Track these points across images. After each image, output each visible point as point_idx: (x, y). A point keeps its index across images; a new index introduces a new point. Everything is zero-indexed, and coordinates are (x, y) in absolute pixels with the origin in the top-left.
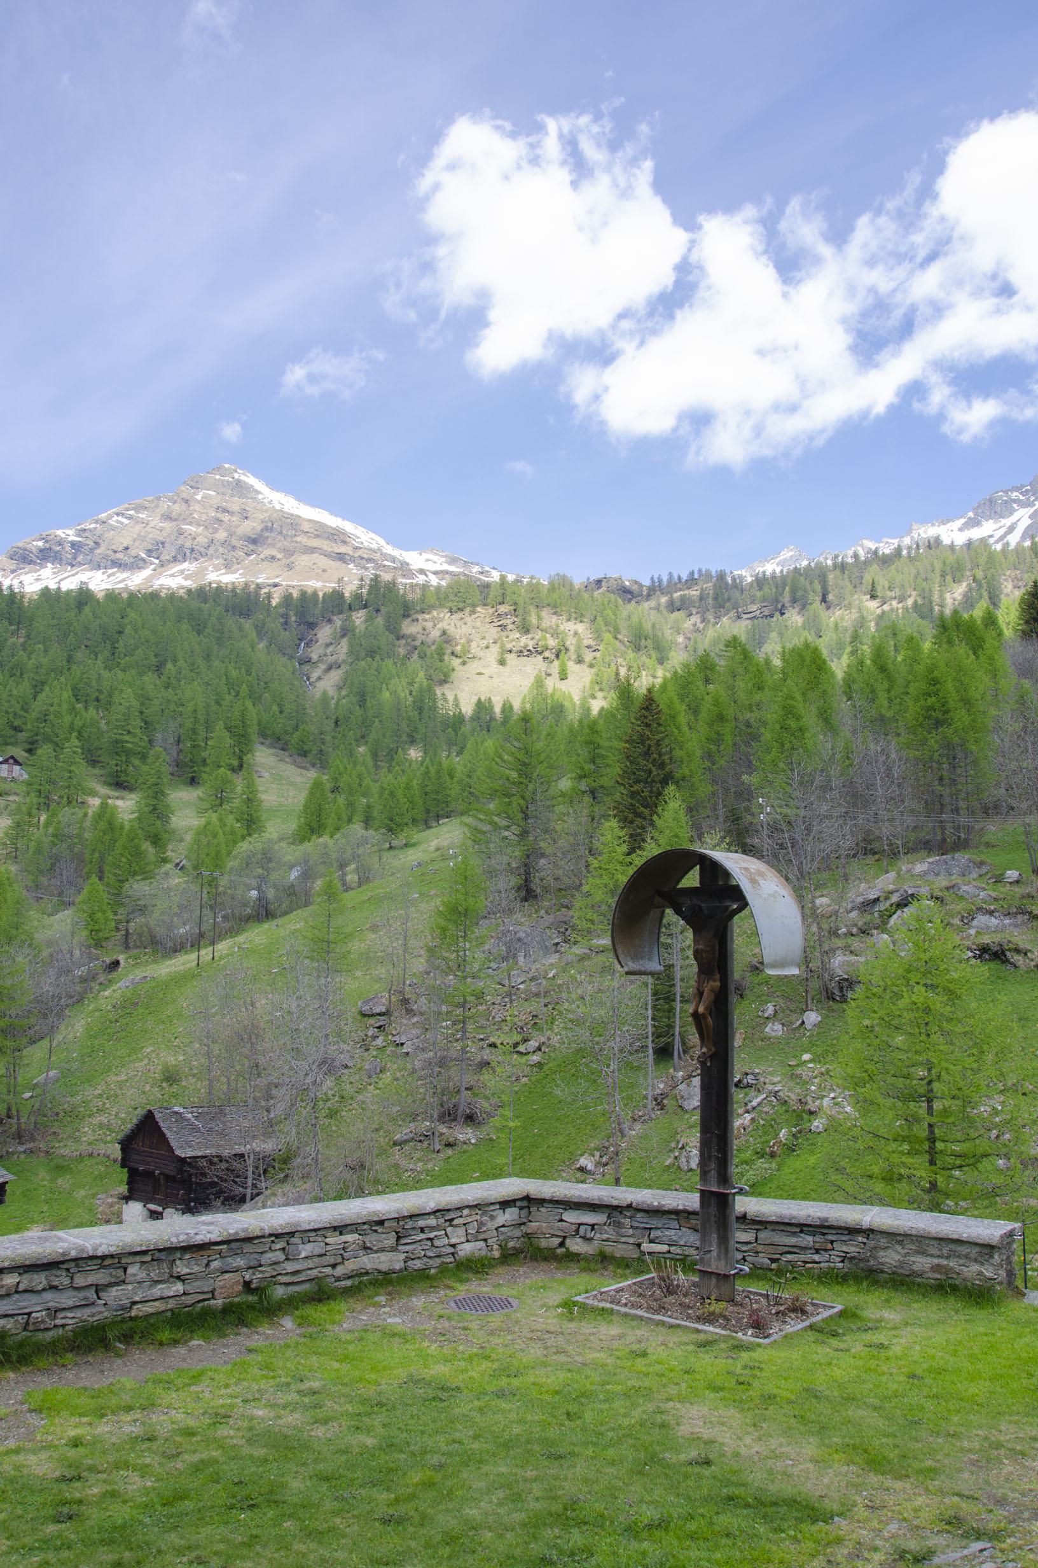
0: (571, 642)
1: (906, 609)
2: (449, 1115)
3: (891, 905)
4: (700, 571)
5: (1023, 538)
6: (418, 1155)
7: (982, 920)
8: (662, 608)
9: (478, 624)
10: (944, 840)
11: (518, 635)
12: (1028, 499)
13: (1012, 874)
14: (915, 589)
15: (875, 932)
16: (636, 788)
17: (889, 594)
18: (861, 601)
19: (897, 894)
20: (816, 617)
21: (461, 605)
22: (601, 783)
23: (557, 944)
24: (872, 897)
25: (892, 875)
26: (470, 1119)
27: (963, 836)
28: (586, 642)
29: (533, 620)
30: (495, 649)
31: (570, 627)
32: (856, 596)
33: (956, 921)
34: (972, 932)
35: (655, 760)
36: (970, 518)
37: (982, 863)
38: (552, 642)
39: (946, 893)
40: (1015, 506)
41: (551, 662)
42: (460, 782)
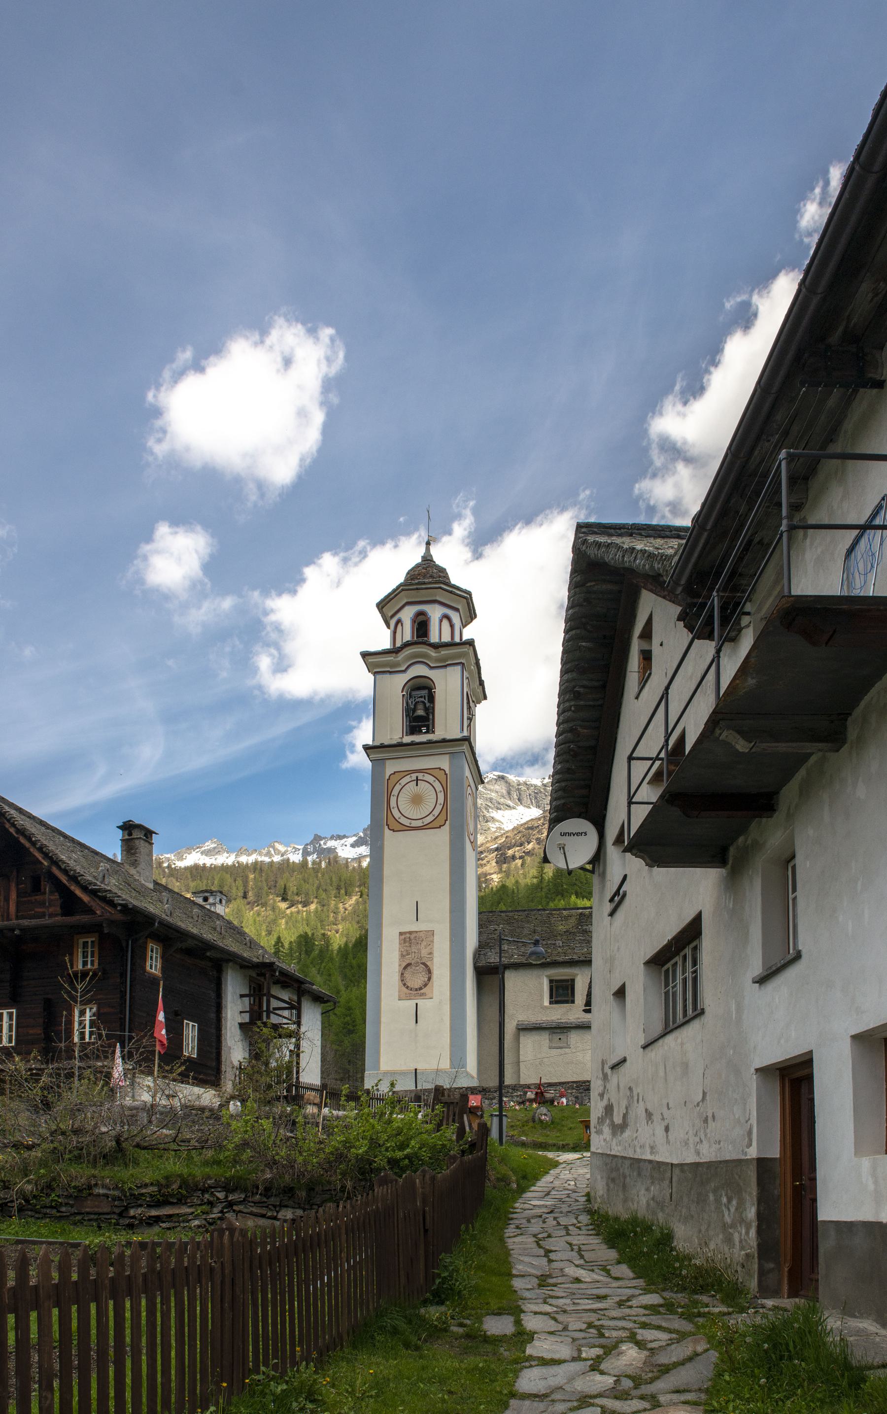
1: (308, 912)
14: (316, 897)
17: (296, 898)
18: (275, 901)
20: (239, 910)
32: (271, 897)
36: (360, 837)
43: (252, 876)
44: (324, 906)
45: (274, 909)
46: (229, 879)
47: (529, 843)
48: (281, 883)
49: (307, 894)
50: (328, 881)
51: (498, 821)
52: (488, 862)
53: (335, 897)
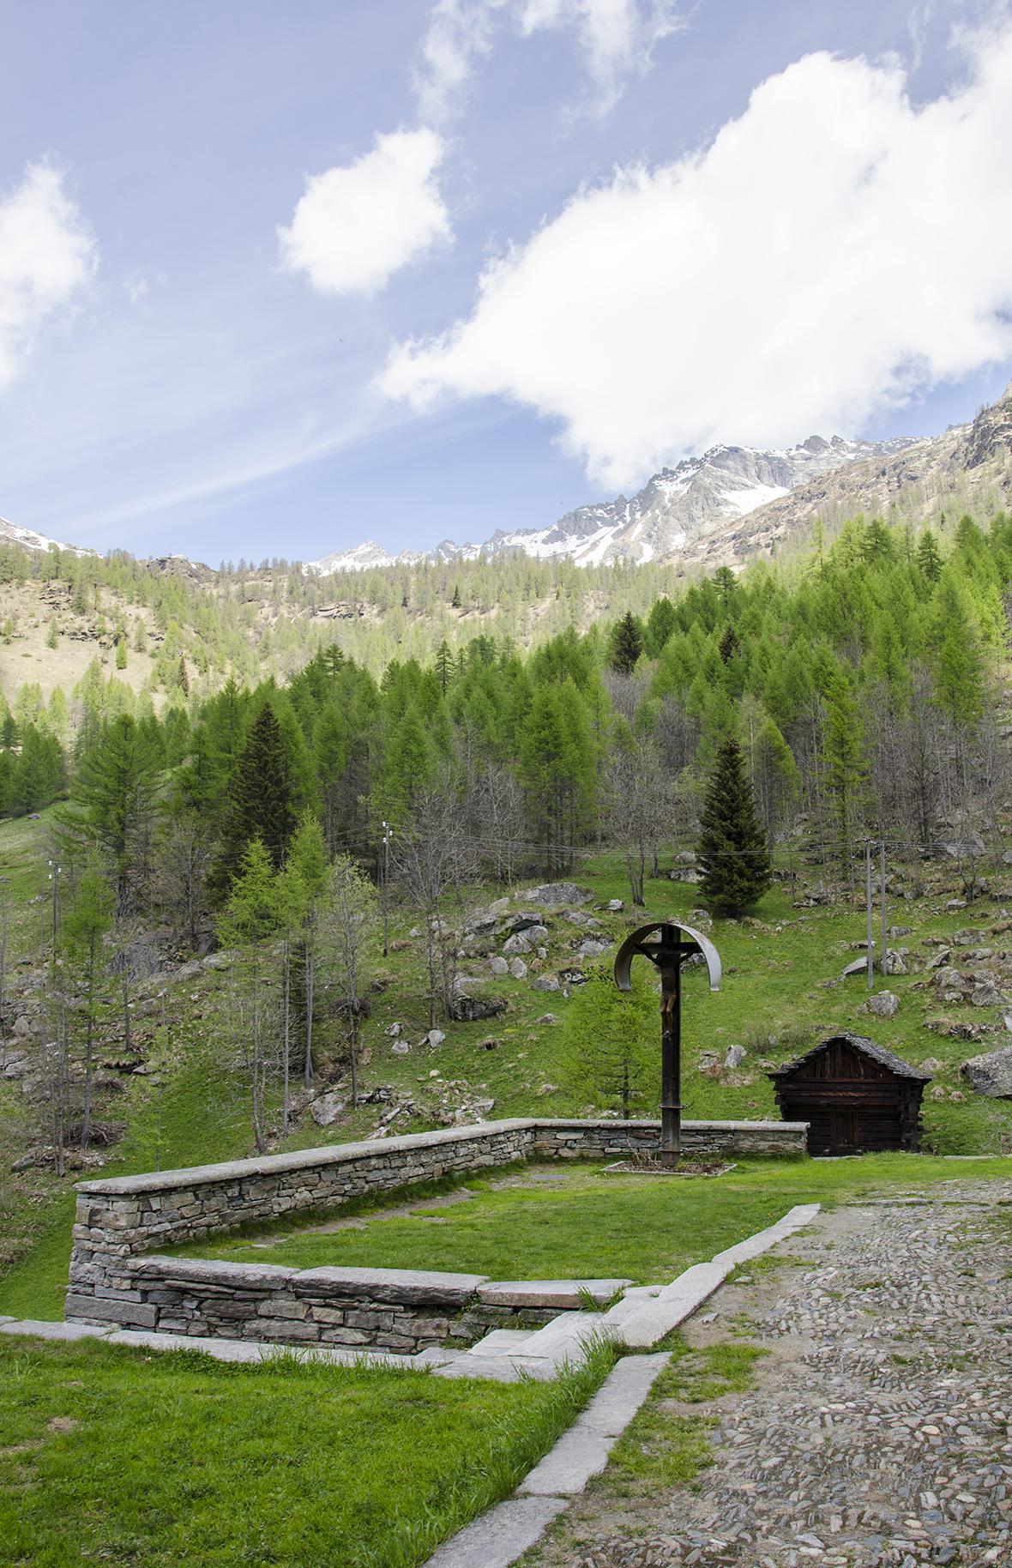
0: (132, 628)
1: (488, 621)
2: (73, 1139)
3: (507, 929)
4: (275, 560)
5: (605, 557)
6: (41, 1180)
7: (589, 945)
8: (231, 597)
9: (27, 599)
10: (550, 868)
11: (72, 616)
12: (612, 518)
13: (616, 903)
15: (491, 955)
16: (250, 804)
17: (472, 603)
18: (443, 608)
19: (513, 919)
20: (396, 621)
21: (8, 576)
22: (207, 796)
23: (162, 962)
24: (488, 921)
25: (505, 901)
26: (97, 1141)
27: (566, 863)
28: (149, 630)
29: (90, 599)
30: (46, 629)
31: (131, 610)
32: (438, 603)
33: (566, 946)
34: (581, 956)
35: (272, 776)
36: (554, 531)
37: (588, 891)
38: (110, 627)
39: (556, 919)
40: (599, 523)
41: (108, 649)
42: (17, 780)
43: (413, 579)
44: (508, 611)
45: (442, 618)
46: (383, 580)
47: (777, 527)
48: (451, 585)
49: (486, 597)
50: (514, 579)
51: (732, 504)
52: (724, 553)
53: (523, 600)
